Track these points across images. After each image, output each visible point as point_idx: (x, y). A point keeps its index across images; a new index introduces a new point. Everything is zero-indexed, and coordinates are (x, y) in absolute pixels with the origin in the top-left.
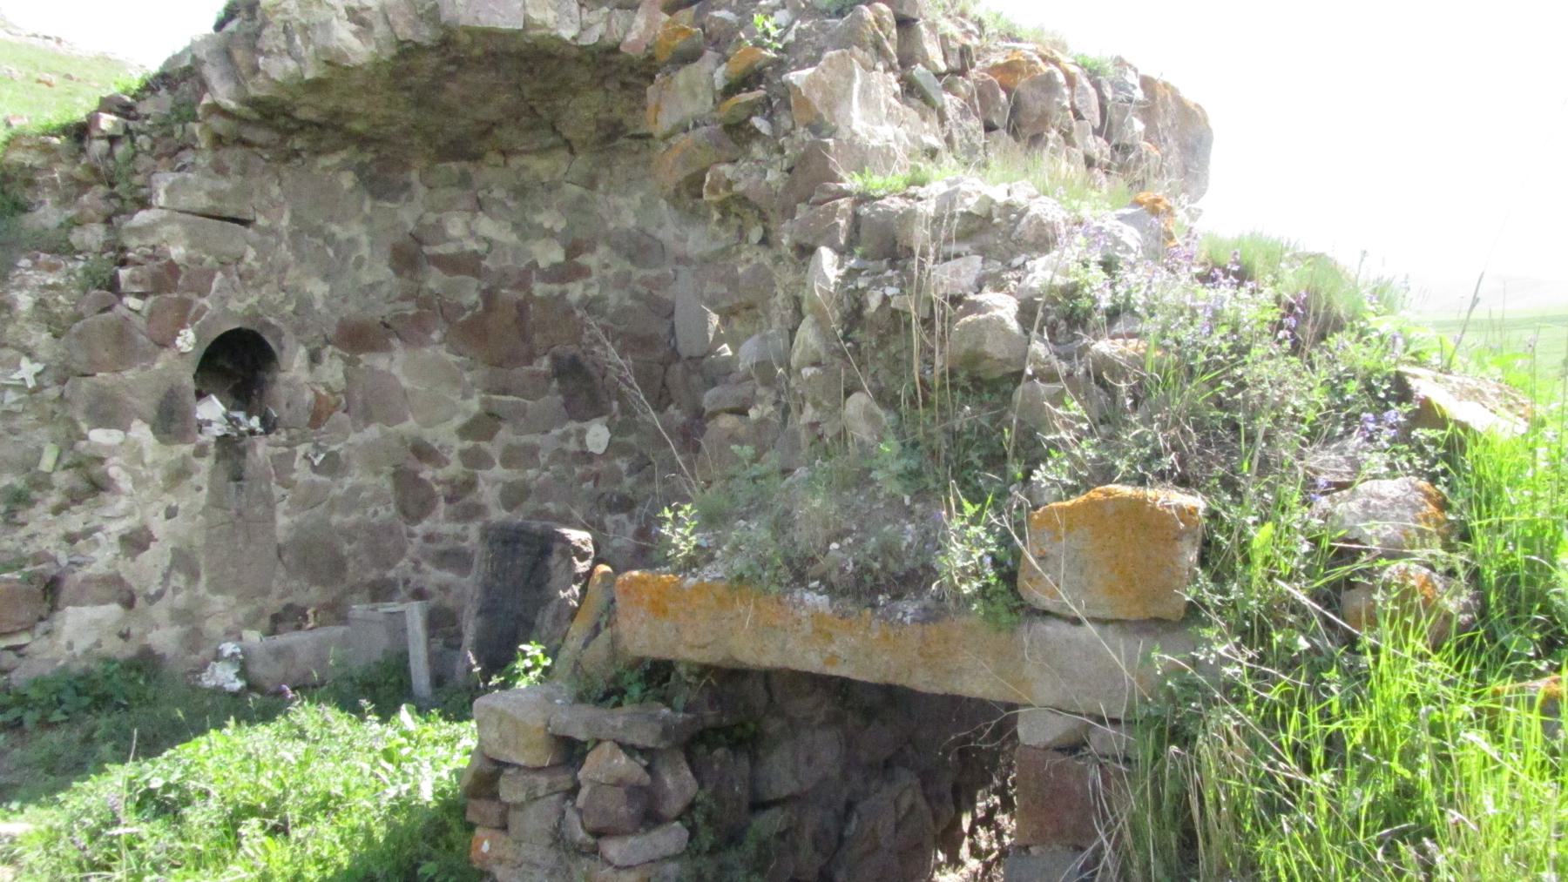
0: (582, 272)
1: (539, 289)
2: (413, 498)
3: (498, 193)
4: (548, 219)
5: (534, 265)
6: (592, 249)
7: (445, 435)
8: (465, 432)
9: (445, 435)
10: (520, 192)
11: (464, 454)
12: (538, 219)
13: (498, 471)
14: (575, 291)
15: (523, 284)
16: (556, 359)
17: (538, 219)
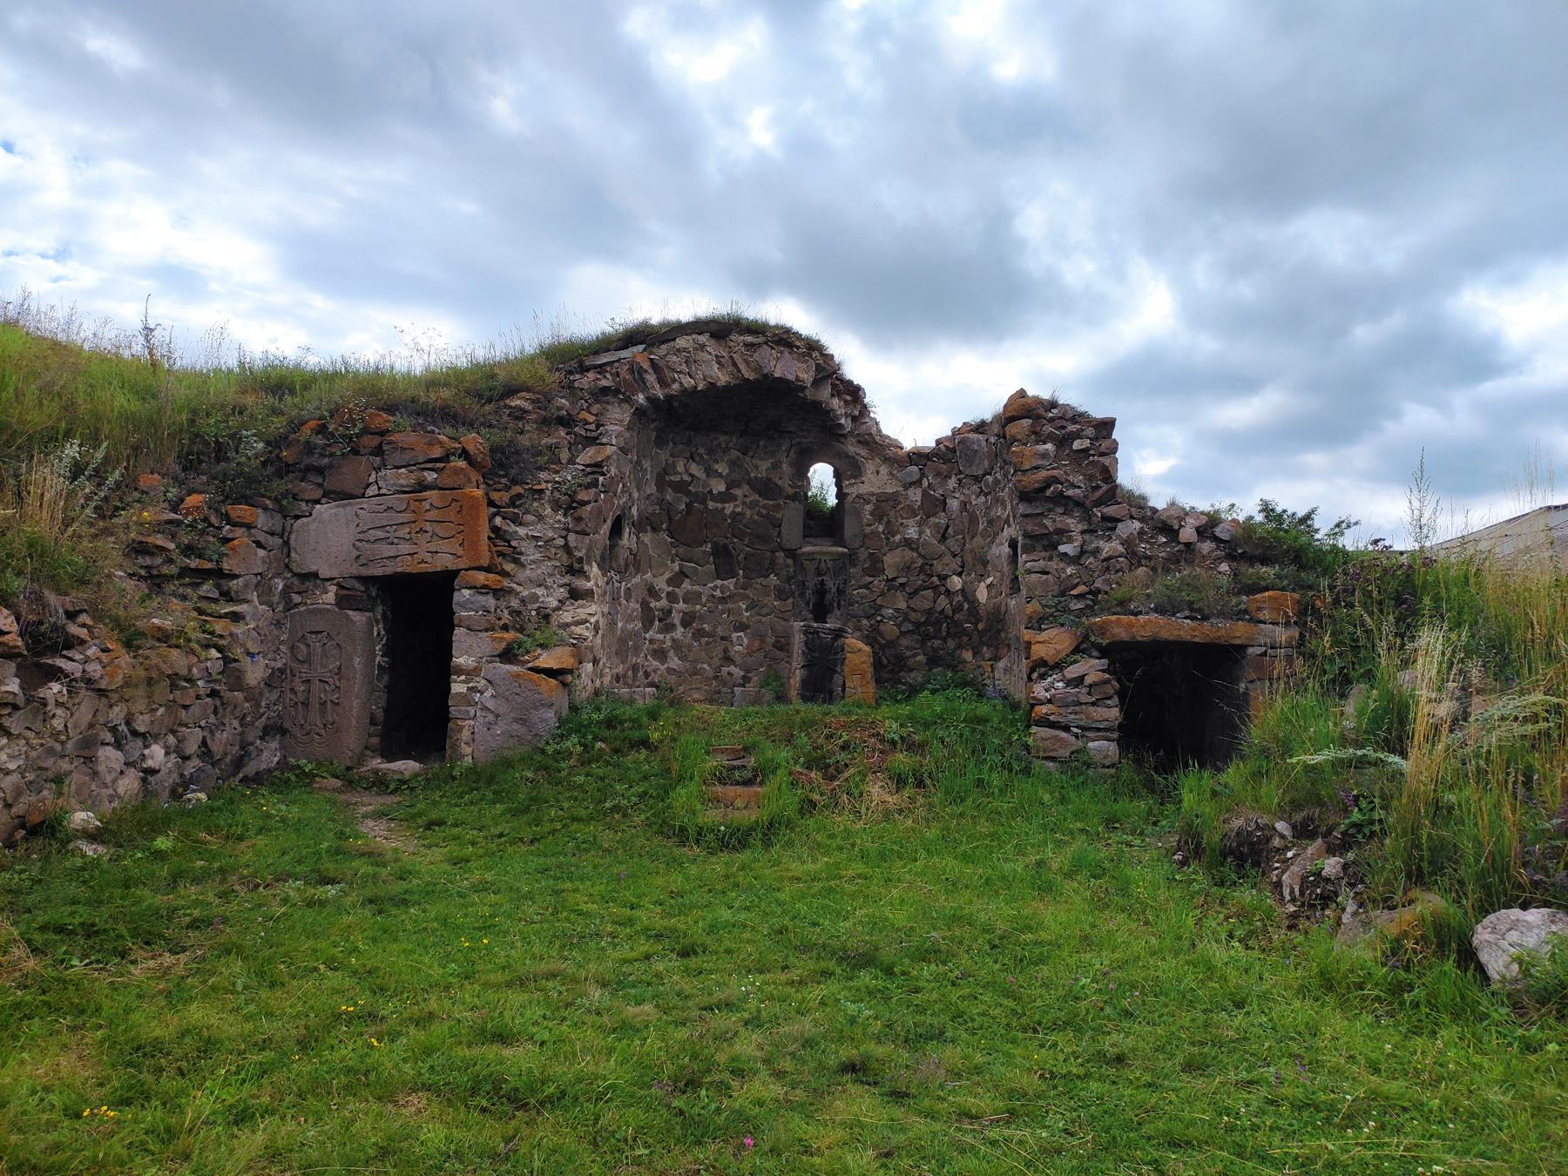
0: (734, 498)
1: (711, 505)
2: (648, 618)
3: (701, 451)
4: (722, 468)
5: (710, 492)
6: (739, 486)
7: (661, 584)
8: (669, 582)
9: (661, 584)
10: (710, 451)
11: (668, 594)
12: (716, 466)
13: (682, 605)
14: (729, 508)
15: (704, 502)
16: (715, 545)
17: (716, 466)
